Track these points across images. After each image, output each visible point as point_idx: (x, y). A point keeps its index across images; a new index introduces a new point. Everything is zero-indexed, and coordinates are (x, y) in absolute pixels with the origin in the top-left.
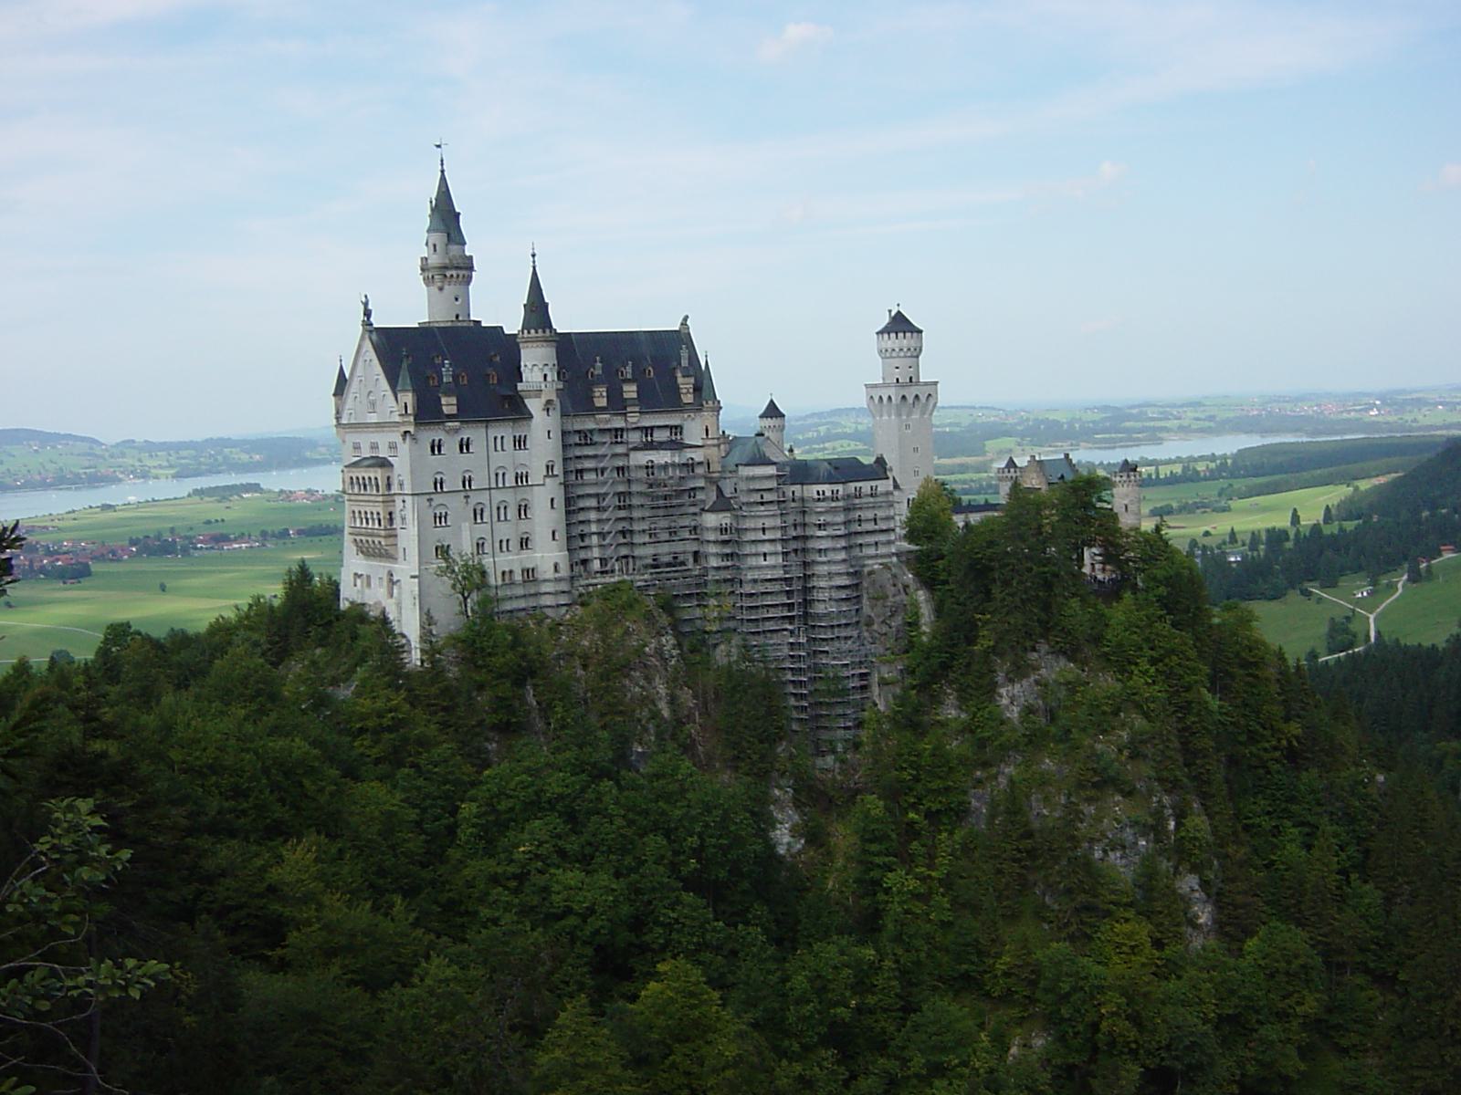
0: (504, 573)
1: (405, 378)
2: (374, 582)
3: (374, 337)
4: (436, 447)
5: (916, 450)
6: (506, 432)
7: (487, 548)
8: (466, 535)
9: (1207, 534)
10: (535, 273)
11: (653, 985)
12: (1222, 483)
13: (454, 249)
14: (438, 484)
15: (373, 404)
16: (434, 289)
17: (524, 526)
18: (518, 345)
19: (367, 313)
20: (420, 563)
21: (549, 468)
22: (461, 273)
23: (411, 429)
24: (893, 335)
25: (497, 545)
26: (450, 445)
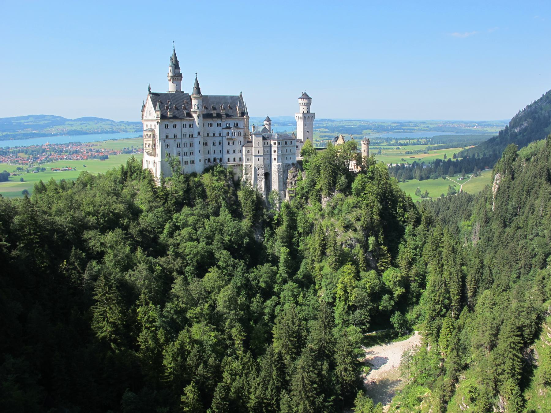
0: (185, 162)
1: (158, 108)
2: (151, 162)
3: (151, 95)
4: (167, 127)
5: (308, 132)
6: (187, 123)
7: (181, 155)
8: (175, 151)
9: (420, 160)
10: (196, 79)
11: (207, 274)
12: (428, 146)
13: (177, 71)
14: (167, 137)
15: (150, 114)
16: (171, 83)
17: (192, 149)
18: (191, 99)
19: (150, 89)
20: (162, 158)
21: (199, 134)
22: (178, 78)
23: (159, 121)
24: (303, 100)
25: (183, 154)
26: (171, 126)
